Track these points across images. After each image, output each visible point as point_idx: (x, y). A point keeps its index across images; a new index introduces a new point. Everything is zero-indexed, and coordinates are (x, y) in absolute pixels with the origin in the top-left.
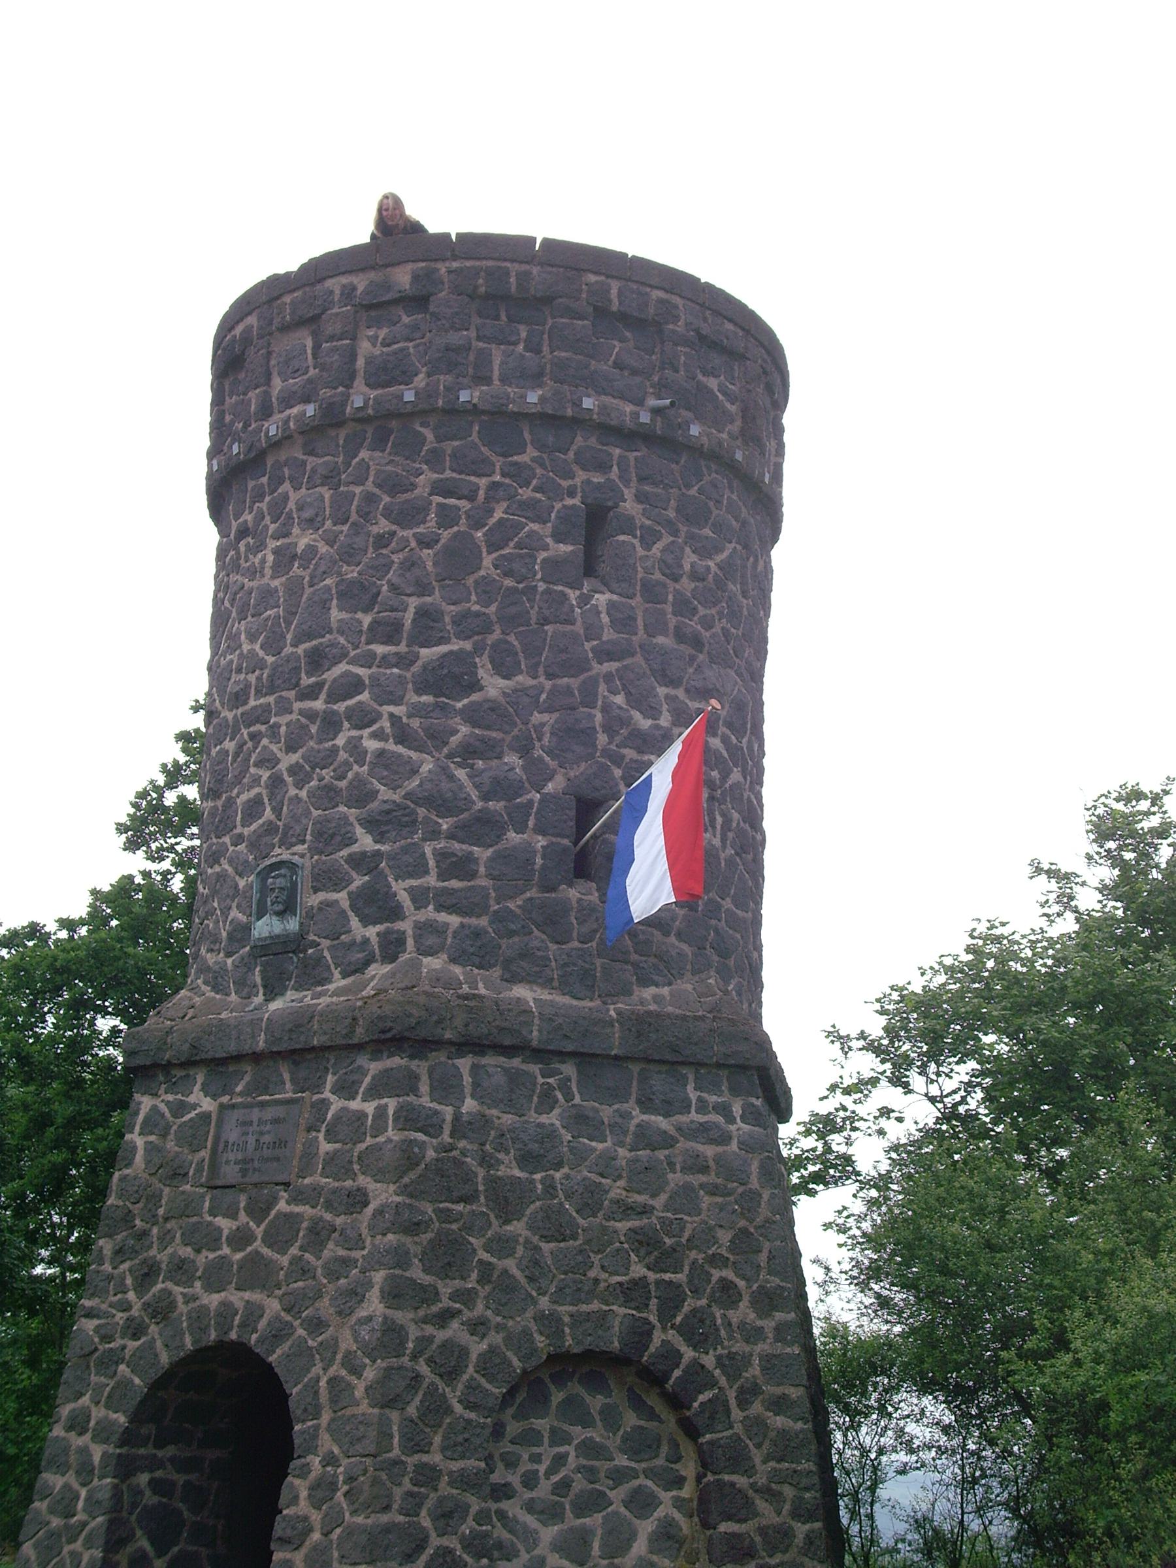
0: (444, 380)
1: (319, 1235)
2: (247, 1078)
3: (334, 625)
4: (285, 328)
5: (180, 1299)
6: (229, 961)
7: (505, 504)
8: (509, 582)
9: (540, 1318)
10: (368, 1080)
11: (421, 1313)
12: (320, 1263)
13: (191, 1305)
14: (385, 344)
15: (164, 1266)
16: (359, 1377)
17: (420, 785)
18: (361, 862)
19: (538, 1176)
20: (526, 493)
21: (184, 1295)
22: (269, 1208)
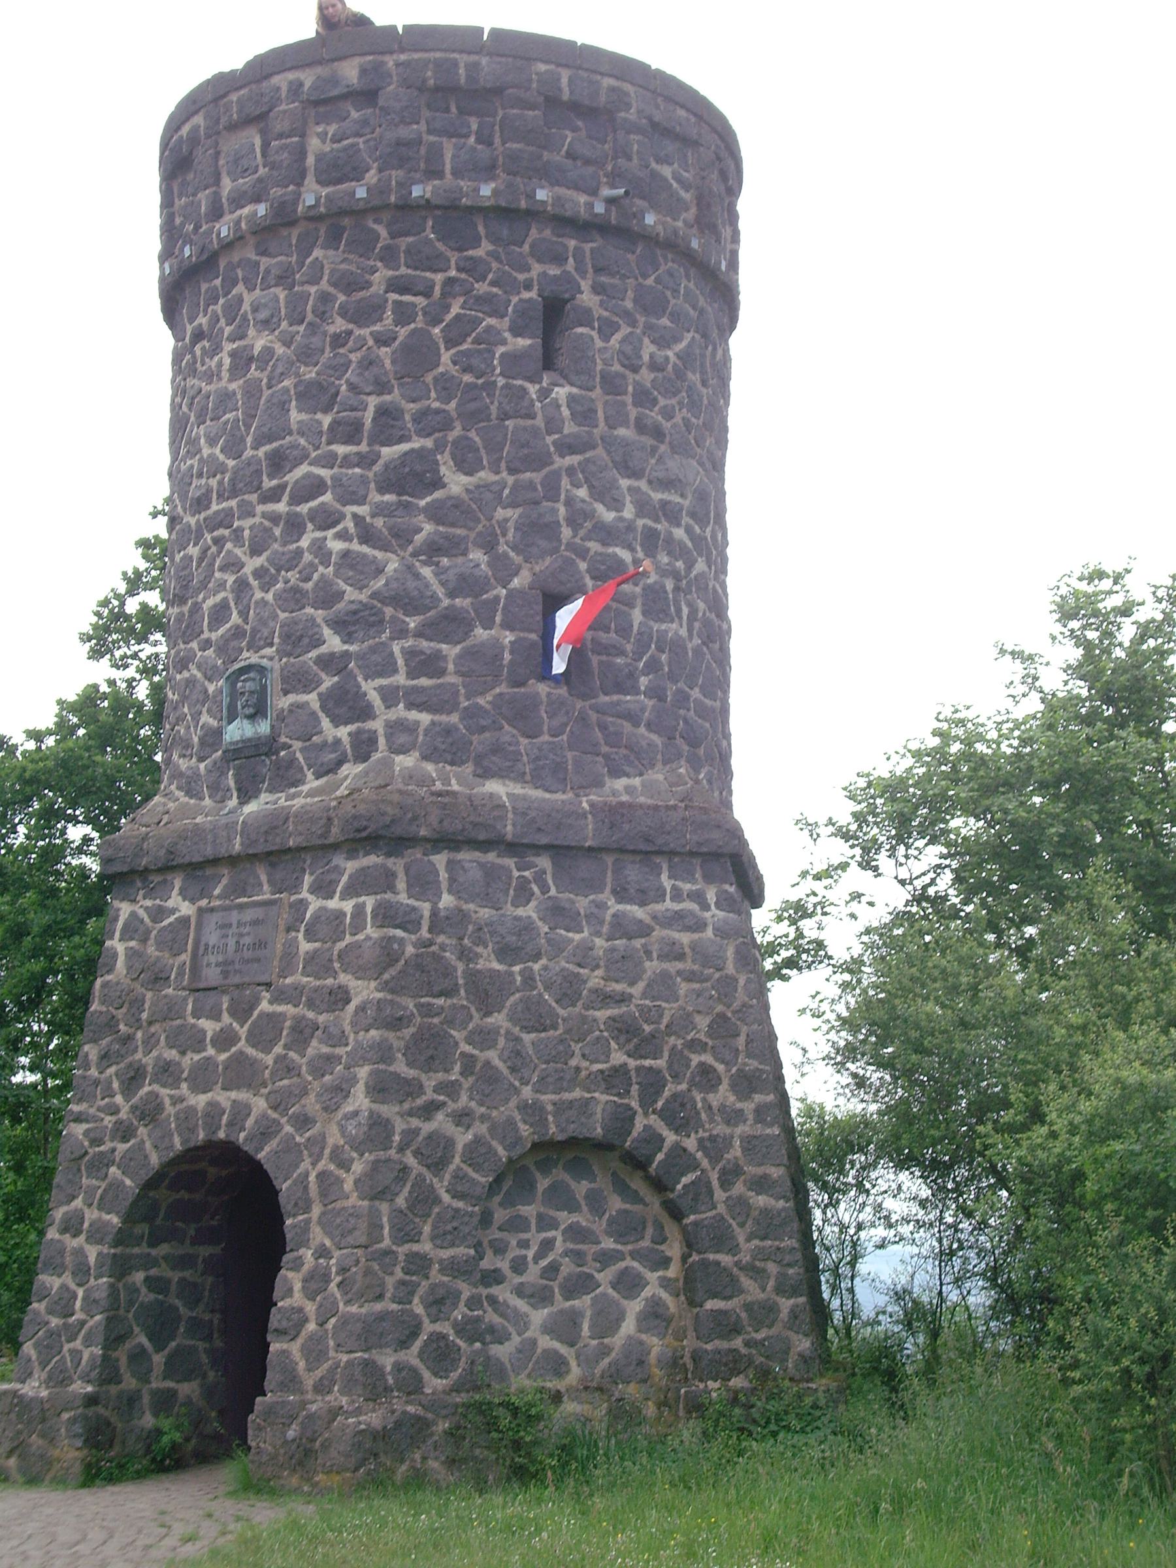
0: (396, 175)
1: (302, 1033)
2: (224, 881)
3: (294, 427)
4: (233, 127)
5: (167, 1101)
6: (202, 766)
7: (462, 300)
8: (467, 378)
9: (523, 1107)
10: (345, 879)
11: (406, 1106)
12: (304, 1060)
13: (178, 1107)
14: (334, 141)
15: (150, 1069)
16: (348, 1170)
17: (386, 584)
18: (329, 663)
19: (517, 968)
20: (482, 288)
21: (171, 1097)
22: (252, 1008)
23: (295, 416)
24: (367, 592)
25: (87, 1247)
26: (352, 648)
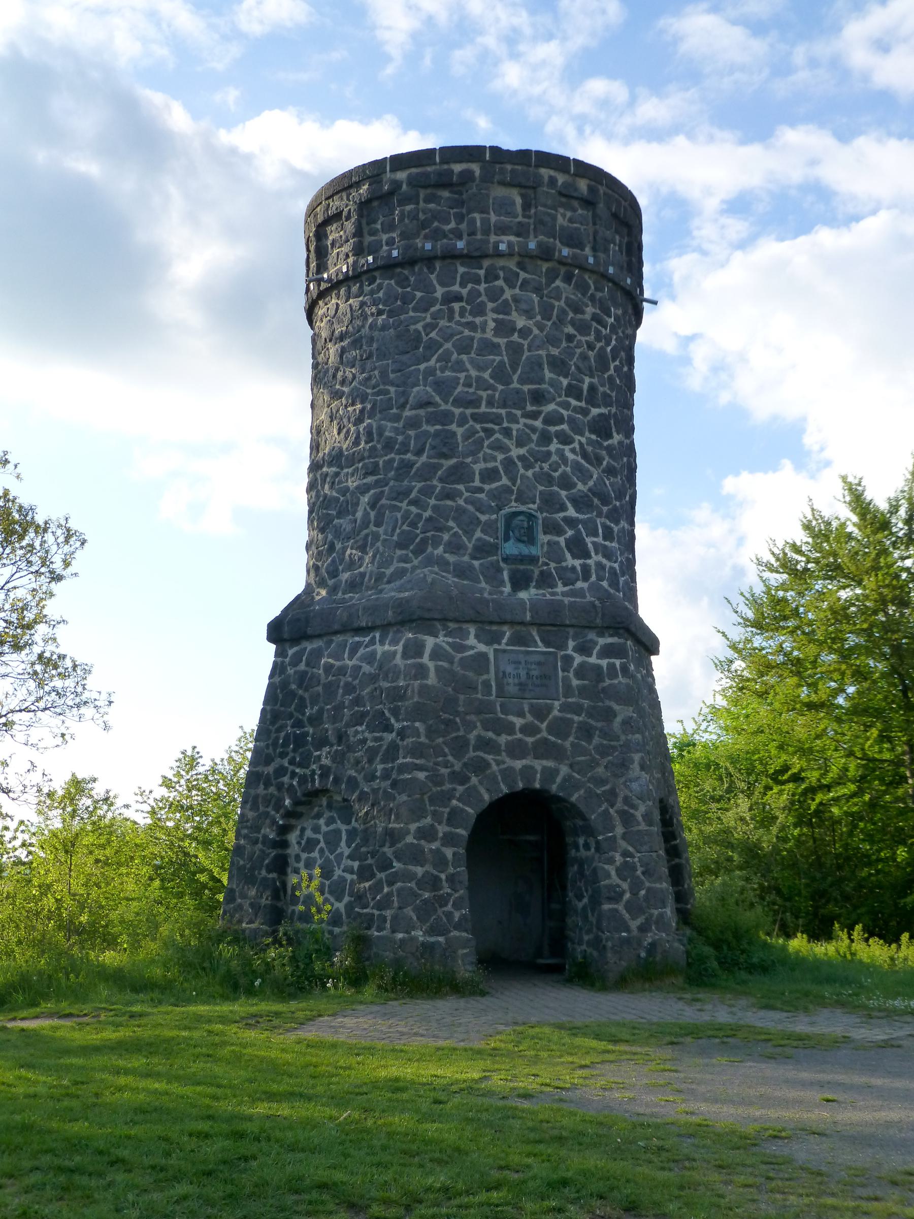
1: (586, 732)
6: (476, 563)
10: (598, 647)
12: (591, 747)
17: (595, 485)
21: (495, 760)
22: (549, 713)
23: (548, 374)
24: (587, 487)
25: (444, 849)
26: (581, 517)
